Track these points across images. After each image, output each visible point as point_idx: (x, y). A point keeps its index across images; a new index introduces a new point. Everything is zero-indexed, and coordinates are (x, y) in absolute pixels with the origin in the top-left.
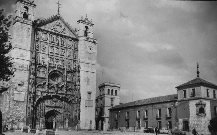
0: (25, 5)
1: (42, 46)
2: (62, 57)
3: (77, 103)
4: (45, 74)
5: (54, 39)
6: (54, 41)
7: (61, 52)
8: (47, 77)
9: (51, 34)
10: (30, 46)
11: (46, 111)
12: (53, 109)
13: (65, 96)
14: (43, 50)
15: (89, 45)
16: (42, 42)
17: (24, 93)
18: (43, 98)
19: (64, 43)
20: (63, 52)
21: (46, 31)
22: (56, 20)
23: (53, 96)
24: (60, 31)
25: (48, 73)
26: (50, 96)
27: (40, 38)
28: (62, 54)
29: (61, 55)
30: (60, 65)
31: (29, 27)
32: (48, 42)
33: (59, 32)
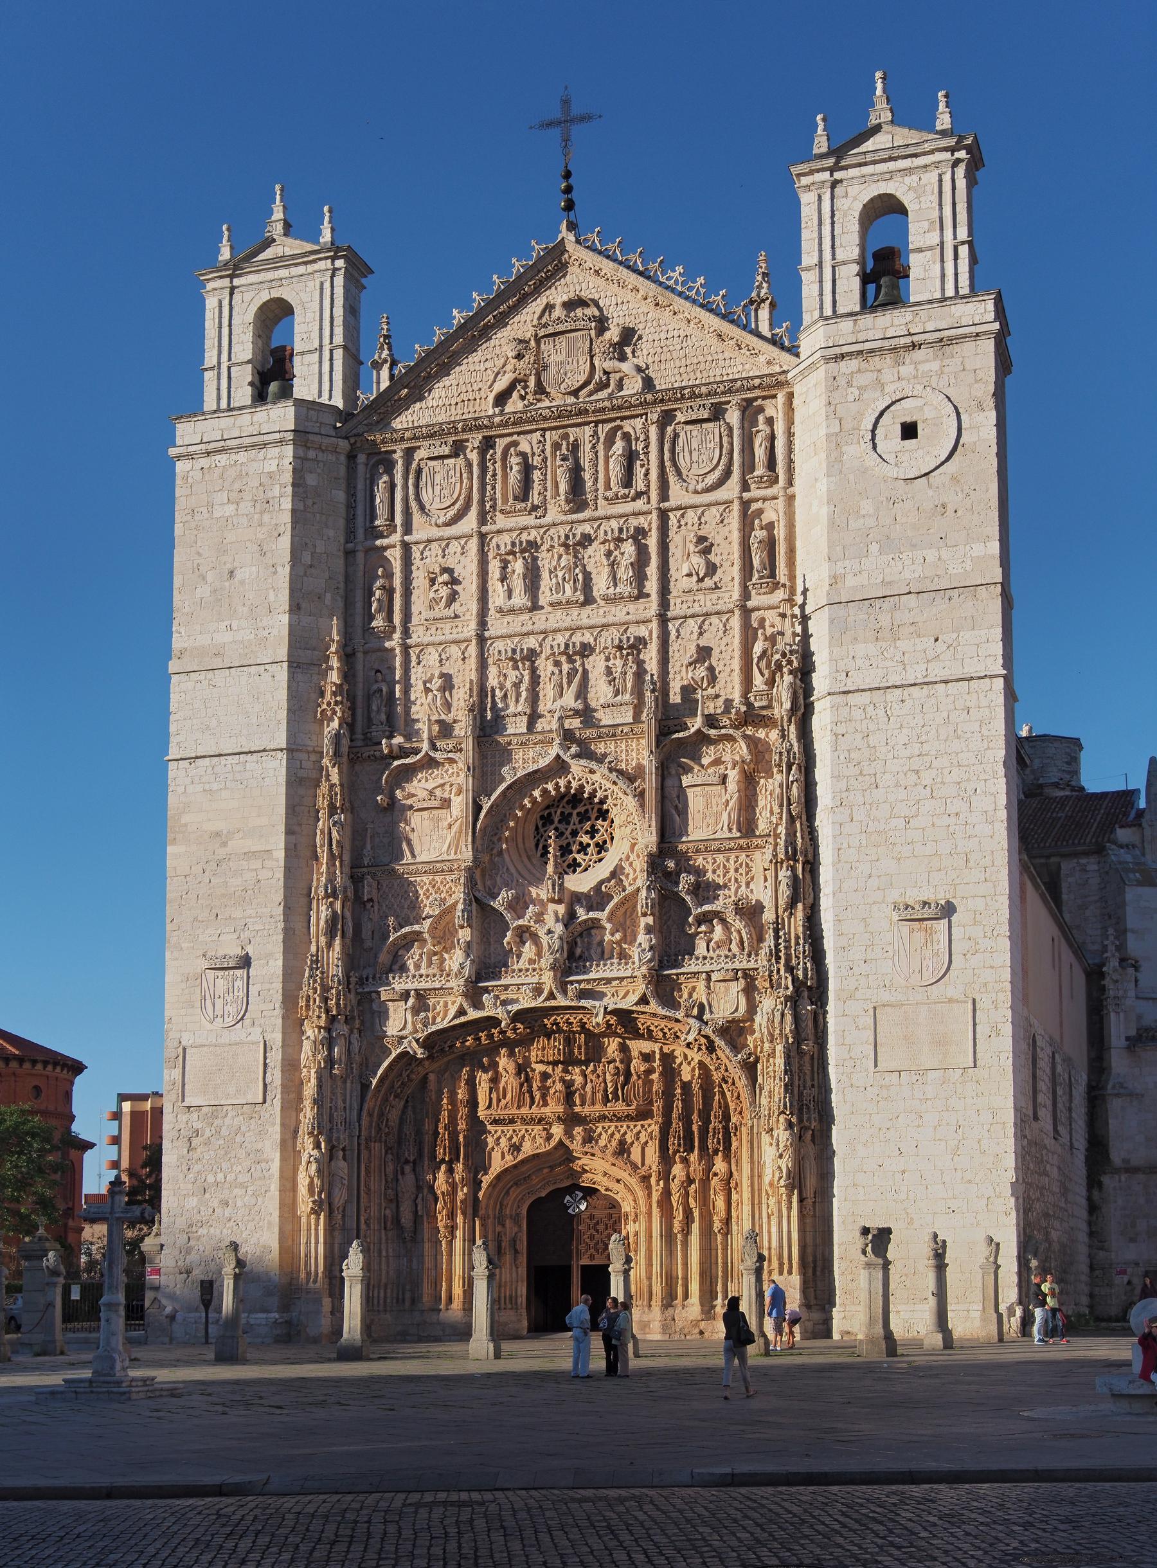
0: (265, 296)
1: (419, 579)
2: (618, 613)
3: (772, 1054)
4: (455, 828)
5: (536, 475)
6: (535, 498)
7: (606, 571)
8: (466, 854)
9: (501, 443)
10: (285, 618)
11: (497, 1164)
12: (553, 1143)
13: (644, 1000)
14: (440, 611)
15: (893, 390)
16: (417, 543)
17: (256, 1035)
18: (420, 1053)
19: (639, 472)
20: (625, 573)
21: (434, 433)
22: (537, 291)
23: (519, 1016)
24: (582, 378)
25: (477, 808)
26: (493, 1021)
27: (399, 519)
28: (623, 589)
29: (609, 600)
30: (602, 701)
31: (271, 466)
32: (470, 522)
33: (575, 393)
